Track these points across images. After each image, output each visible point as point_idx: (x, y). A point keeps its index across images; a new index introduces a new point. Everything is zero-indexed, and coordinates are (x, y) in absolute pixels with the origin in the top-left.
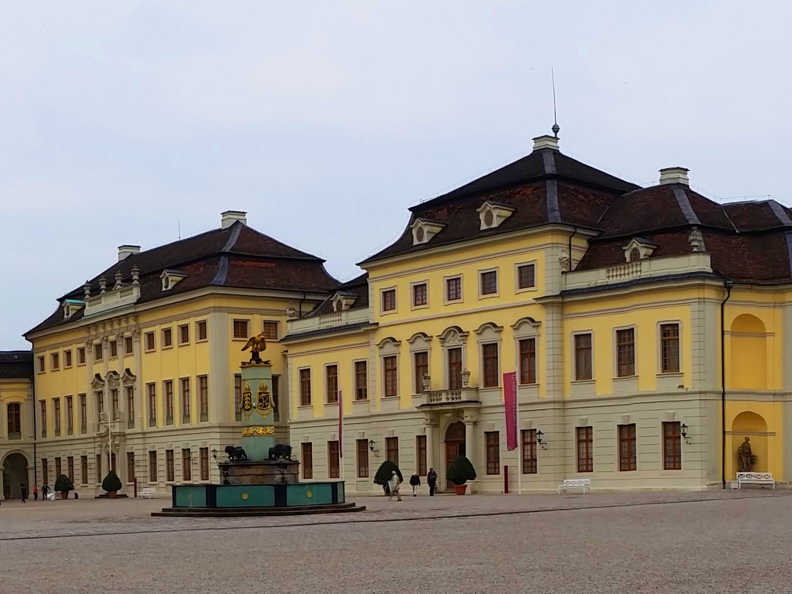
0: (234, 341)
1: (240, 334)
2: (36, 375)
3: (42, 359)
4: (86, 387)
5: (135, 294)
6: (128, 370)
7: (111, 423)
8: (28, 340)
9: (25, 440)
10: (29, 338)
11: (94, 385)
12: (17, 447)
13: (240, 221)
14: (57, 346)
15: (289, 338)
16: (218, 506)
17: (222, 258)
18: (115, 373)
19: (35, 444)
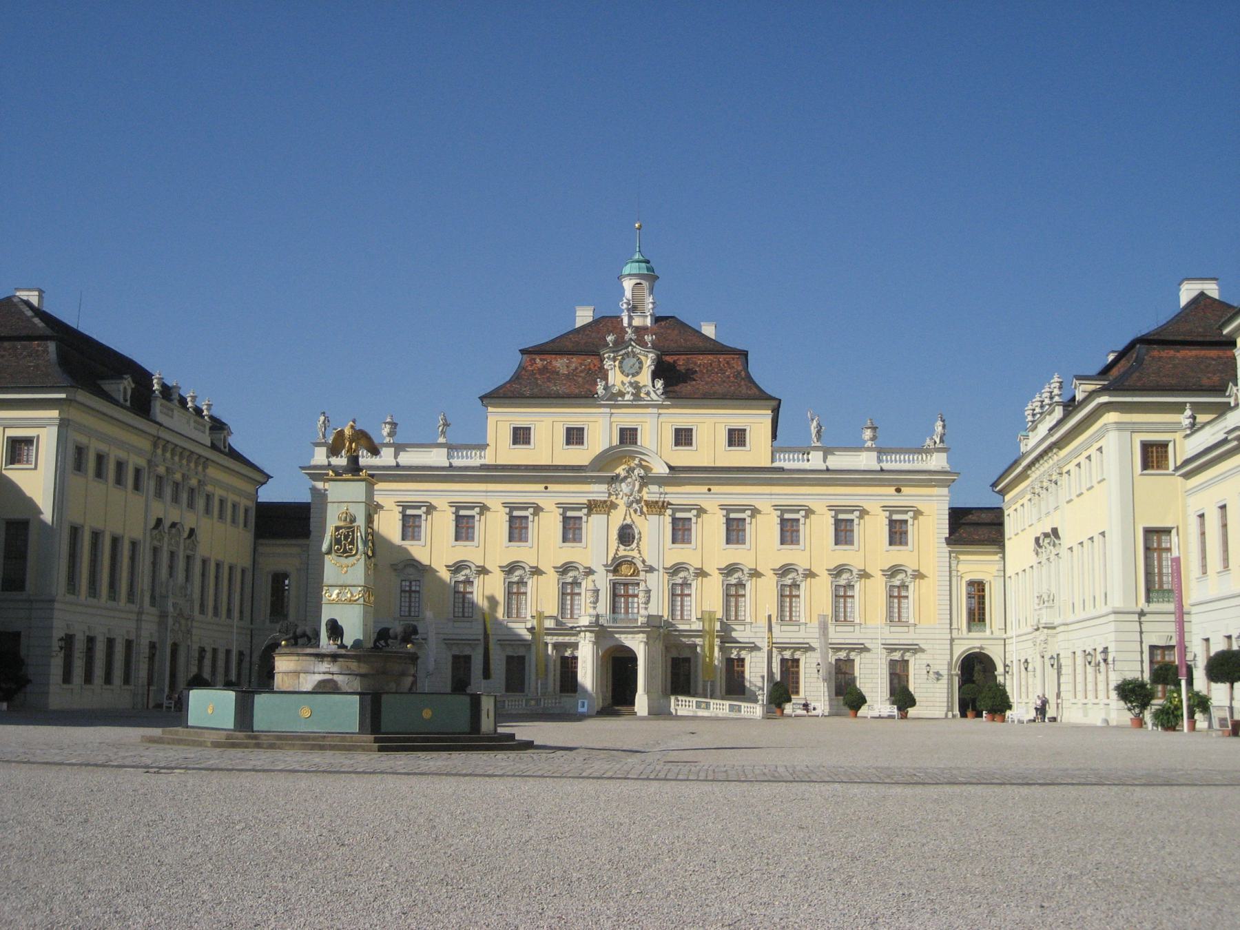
0: (1141, 475)
1: (1155, 464)
2: (1006, 541)
3: (1009, 515)
4: (1033, 560)
5: (1058, 413)
6: (1055, 531)
7: (637, 596)
8: (997, 492)
9: (992, 633)
10: (998, 488)
11: (1037, 554)
12: (977, 644)
13: (1206, 292)
14: (1014, 500)
15: (1187, 462)
16: (189, 724)
17: (1138, 346)
18: (1046, 535)
19: (1005, 640)
